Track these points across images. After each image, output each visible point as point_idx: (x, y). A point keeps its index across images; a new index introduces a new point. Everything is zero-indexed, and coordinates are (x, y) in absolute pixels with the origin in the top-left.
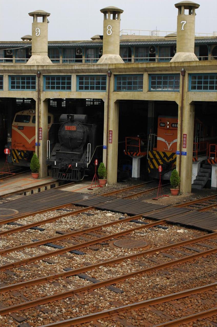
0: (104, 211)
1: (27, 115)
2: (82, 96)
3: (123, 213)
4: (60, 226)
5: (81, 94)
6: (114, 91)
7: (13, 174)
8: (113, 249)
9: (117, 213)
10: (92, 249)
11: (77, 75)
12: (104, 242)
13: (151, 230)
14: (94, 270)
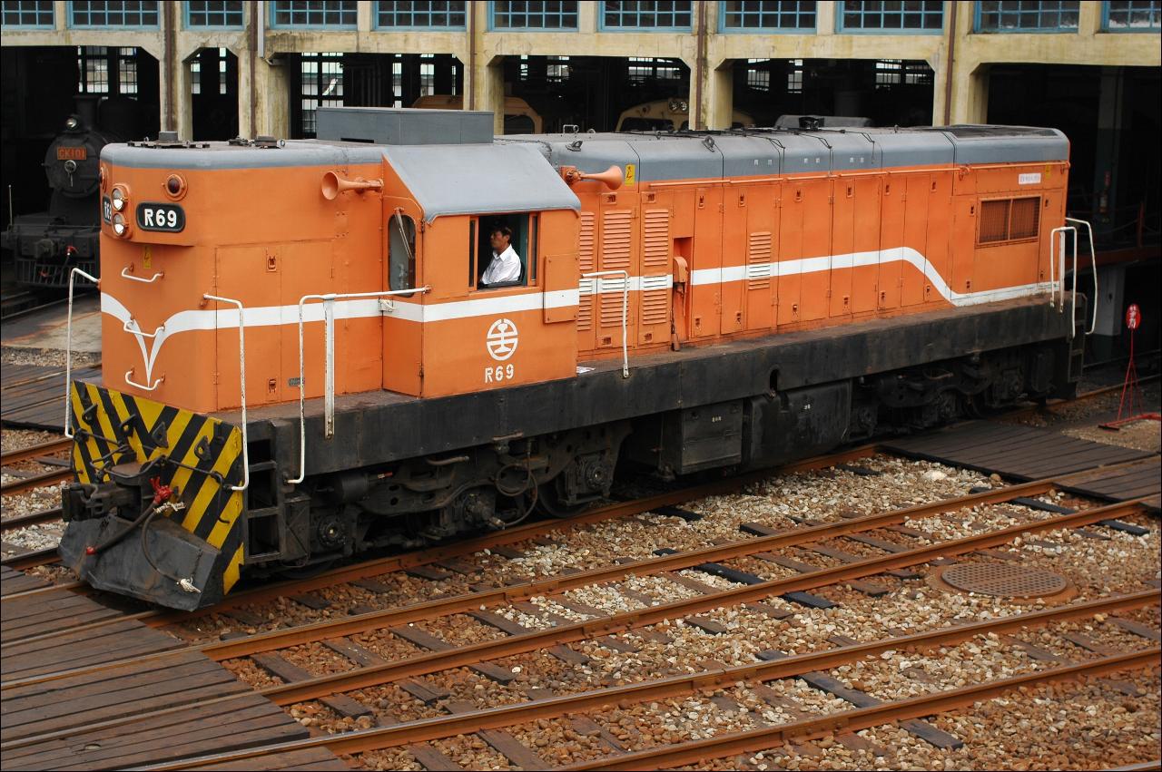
0: (917, 463)
1: (660, 117)
2: (854, 49)
3: (986, 473)
4: (756, 508)
5: (851, 41)
6: (973, 31)
8: (938, 596)
9: (964, 471)
10: (862, 592)
12: (907, 570)
13: (1083, 536)
14: (864, 662)
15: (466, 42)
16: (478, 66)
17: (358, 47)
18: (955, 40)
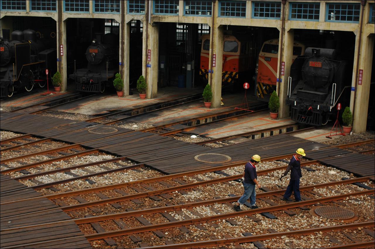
0: (329, 168)
1: (276, 44)
2: (331, 27)
3: (350, 173)
4: (268, 181)
5: (330, 24)
7: (251, 112)
8: (311, 217)
9: (343, 172)
10: (287, 214)
11: (326, 3)
12: (306, 207)
13: (370, 198)
14: (275, 239)
15: (211, 20)
16: (215, 28)
17: (179, 21)
18: (363, 25)
